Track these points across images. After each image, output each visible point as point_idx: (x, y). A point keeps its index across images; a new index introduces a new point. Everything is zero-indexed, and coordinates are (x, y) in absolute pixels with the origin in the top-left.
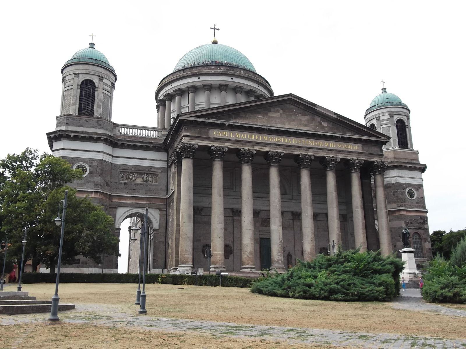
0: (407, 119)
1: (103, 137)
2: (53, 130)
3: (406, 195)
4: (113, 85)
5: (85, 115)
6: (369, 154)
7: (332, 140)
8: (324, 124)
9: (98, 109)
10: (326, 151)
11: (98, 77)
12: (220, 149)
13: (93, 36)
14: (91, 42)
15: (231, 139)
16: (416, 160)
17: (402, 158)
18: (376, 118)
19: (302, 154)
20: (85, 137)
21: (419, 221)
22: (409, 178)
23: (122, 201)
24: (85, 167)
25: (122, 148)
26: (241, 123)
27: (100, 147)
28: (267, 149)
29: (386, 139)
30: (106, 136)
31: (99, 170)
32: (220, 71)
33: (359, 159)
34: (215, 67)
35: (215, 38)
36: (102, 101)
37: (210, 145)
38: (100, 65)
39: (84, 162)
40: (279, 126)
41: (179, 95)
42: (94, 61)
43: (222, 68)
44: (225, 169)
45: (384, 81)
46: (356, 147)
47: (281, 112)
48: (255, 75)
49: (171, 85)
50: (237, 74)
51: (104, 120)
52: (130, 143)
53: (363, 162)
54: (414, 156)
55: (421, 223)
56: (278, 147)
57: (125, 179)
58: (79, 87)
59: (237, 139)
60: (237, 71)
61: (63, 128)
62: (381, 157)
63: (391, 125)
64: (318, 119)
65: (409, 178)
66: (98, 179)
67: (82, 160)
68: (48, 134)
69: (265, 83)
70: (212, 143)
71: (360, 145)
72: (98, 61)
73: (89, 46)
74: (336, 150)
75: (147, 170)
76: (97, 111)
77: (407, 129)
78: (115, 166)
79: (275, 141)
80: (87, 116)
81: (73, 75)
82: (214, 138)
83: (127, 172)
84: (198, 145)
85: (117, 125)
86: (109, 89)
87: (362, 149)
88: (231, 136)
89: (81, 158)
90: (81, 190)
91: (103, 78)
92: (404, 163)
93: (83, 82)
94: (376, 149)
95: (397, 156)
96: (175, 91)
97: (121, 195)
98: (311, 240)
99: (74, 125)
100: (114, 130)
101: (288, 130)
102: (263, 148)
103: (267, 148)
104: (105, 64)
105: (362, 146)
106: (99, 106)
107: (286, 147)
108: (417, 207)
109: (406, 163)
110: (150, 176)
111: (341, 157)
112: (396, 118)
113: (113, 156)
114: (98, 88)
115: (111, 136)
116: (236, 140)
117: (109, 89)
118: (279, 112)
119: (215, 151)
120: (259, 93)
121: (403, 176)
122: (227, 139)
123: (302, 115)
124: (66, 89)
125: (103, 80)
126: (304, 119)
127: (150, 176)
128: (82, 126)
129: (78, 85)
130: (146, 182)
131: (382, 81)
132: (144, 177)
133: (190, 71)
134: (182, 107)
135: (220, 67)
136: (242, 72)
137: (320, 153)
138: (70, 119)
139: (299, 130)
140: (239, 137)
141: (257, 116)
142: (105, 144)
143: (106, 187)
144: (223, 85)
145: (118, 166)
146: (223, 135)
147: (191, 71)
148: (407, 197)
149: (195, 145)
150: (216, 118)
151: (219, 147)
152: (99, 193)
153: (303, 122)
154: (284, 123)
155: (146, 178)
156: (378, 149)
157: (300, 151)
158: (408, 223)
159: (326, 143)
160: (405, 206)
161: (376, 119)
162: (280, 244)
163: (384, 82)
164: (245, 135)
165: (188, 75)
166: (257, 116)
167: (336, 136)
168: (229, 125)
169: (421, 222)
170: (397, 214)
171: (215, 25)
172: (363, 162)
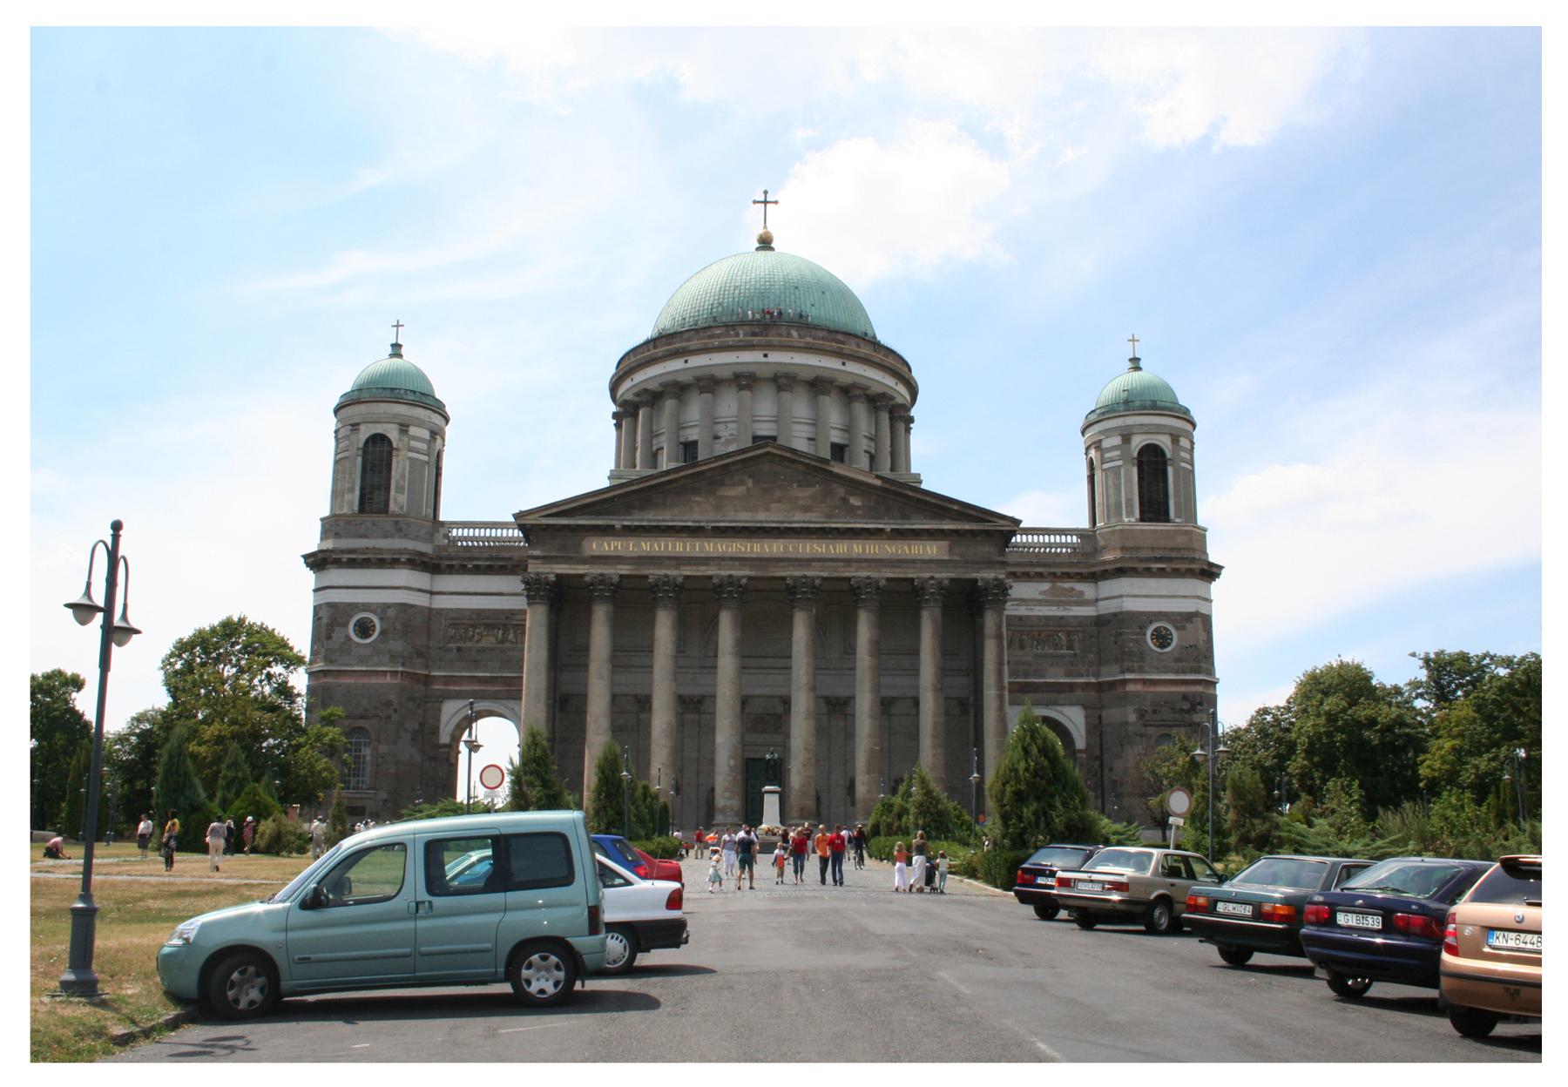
1: (403, 556)
2: (314, 549)
3: (1145, 642)
4: (436, 434)
5: (372, 513)
6: (966, 562)
8: (855, 501)
9: (398, 495)
10: (855, 565)
11: (396, 426)
12: (603, 579)
13: (398, 326)
14: (394, 342)
15: (628, 555)
16: (1184, 549)
17: (1143, 548)
18: (1094, 443)
20: (369, 559)
21: (1178, 707)
22: (1161, 596)
23: (452, 688)
24: (372, 621)
25: (451, 573)
26: (649, 521)
27: (402, 576)
29: (1008, 526)
30: (410, 554)
31: (399, 627)
32: (733, 341)
33: (936, 576)
34: (723, 329)
35: (765, 227)
36: (407, 475)
37: (581, 572)
38: (402, 399)
39: (371, 611)
41: (645, 404)
42: (388, 394)
43: (741, 332)
45: (1136, 338)
46: (932, 549)
47: (750, 483)
48: (833, 335)
49: (630, 378)
50: (776, 343)
52: (465, 563)
53: (946, 582)
54: (1181, 540)
55: (1182, 710)
56: (737, 563)
58: (360, 452)
59: (644, 554)
60: (781, 335)
61: (329, 544)
62: (998, 566)
63: (1124, 463)
64: (841, 491)
65: (1161, 596)
66: (397, 645)
67: (366, 607)
68: (306, 557)
69: (865, 350)
70: (587, 567)
71: (945, 543)
73: (389, 350)
74: (881, 561)
75: (504, 617)
77: (1170, 470)
78: (437, 613)
80: (376, 513)
81: (349, 427)
84: (557, 576)
85: (443, 524)
86: (424, 447)
88: (631, 549)
90: (364, 669)
91: (408, 426)
92: (1141, 560)
93: (367, 442)
94: (986, 549)
95: (1131, 544)
96: (637, 394)
97: (449, 674)
98: (804, 765)
99: (349, 536)
100: (436, 534)
101: (758, 525)
102: (703, 568)
103: (712, 568)
104: (412, 394)
105: (950, 546)
106: (400, 490)
108: (1177, 672)
109: (1149, 560)
110: (512, 631)
112: (1138, 442)
113: (432, 593)
114: (397, 449)
115: (421, 554)
116: (640, 558)
117: (424, 447)
118: (743, 485)
119: (592, 584)
120: (844, 380)
121: (1143, 592)
122: (620, 556)
123: (800, 485)
124: (339, 457)
125: (407, 431)
126: (804, 493)
127: (512, 631)
129: (358, 449)
130: (503, 642)
131: (1131, 338)
133: (666, 345)
134: (655, 434)
135: (737, 328)
136: (794, 333)
137: (839, 569)
138: (342, 523)
139: (783, 522)
141: (693, 499)
142: (412, 569)
143: (418, 661)
144: (742, 376)
145: (443, 612)
146: (612, 549)
147: (670, 344)
148: (1150, 648)
149: (549, 576)
150: (599, 514)
151: (601, 575)
152: (399, 675)
153: (801, 502)
154: (754, 509)
155: (503, 634)
156: (993, 550)
157: (790, 568)
158: (1146, 711)
159: (855, 546)
160: (1141, 670)
161: (1093, 446)
165: (660, 355)
166: (693, 499)
168: (624, 527)
169: (1185, 707)
170: (1119, 690)
171: (766, 192)
172: (946, 582)
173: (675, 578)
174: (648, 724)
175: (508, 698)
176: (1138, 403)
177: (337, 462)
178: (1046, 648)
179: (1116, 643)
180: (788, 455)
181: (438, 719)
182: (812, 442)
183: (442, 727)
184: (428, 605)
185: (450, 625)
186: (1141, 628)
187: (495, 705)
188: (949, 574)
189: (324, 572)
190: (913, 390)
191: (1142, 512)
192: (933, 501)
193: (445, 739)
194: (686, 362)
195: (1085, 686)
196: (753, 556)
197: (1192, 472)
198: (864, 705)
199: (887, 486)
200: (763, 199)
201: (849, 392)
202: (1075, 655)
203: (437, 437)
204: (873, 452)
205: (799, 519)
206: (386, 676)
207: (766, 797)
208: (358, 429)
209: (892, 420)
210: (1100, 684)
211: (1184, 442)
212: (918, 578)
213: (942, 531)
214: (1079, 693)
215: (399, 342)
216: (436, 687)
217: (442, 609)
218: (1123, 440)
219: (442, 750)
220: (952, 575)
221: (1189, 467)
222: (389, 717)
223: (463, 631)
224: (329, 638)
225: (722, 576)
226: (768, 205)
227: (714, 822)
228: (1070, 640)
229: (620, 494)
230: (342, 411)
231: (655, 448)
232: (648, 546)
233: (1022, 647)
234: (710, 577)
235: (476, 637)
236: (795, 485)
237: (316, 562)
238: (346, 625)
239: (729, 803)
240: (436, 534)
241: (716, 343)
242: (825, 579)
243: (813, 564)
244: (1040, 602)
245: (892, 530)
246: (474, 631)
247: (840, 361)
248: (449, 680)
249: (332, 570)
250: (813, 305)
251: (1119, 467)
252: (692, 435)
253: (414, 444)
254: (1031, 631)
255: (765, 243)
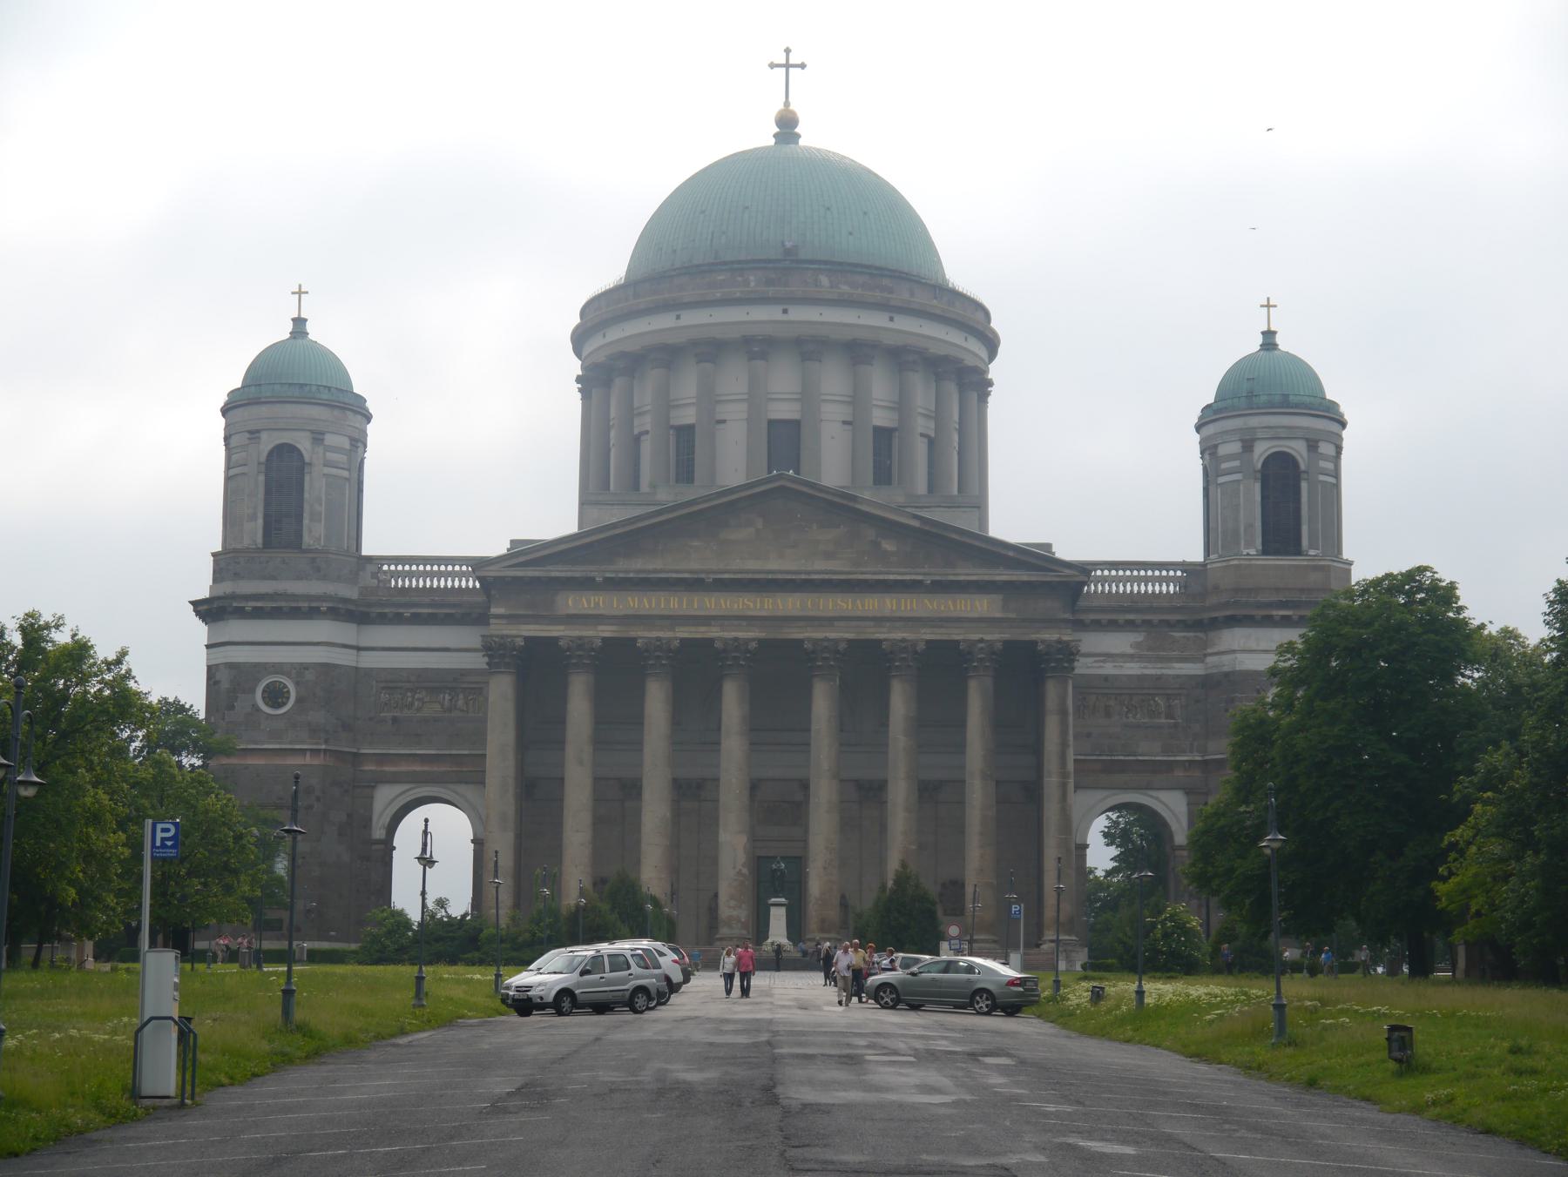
0: (1309, 451)
2: (204, 593)
8: (888, 546)
10: (888, 624)
11: (308, 434)
12: (580, 643)
13: (300, 293)
19: (809, 639)
23: (386, 769)
24: (285, 686)
25: (384, 624)
28: (713, 632)
29: (1076, 576)
36: (324, 498)
39: (282, 673)
40: (752, 565)
43: (752, 278)
44: (600, 697)
46: (982, 605)
51: (330, 556)
52: (401, 611)
56: (744, 623)
57: (395, 708)
58: (263, 468)
59: (630, 612)
61: (227, 587)
67: (278, 668)
68: (195, 603)
70: (562, 628)
71: (997, 598)
72: (308, 388)
76: (310, 531)
77: (1304, 485)
79: (736, 606)
81: (247, 435)
83: (396, 688)
84: (527, 639)
85: (370, 559)
89: (274, 665)
90: (277, 746)
91: (323, 433)
93: (271, 453)
98: (825, 868)
100: (361, 573)
102: (703, 629)
103: (714, 629)
104: (327, 391)
109: (1270, 605)
110: (461, 696)
111: (928, 637)
112: (1262, 450)
114: (310, 464)
115: (345, 601)
116: (626, 617)
119: (569, 649)
124: (232, 472)
125: (323, 440)
127: (461, 696)
128: (273, 578)
129: (259, 463)
130: (450, 710)
132: (444, 698)
134: (635, 412)
136: (824, 280)
140: (636, 606)
146: (592, 605)
151: (580, 638)
155: (451, 700)
162: (736, 880)
163: (1275, 306)
164: (654, 600)
167: (914, 581)
168: (607, 580)
171: (788, 51)
173: (670, 640)
174: (638, 813)
175: (460, 782)
176: (1263, 399)
177: (228, 479)
178: (1138, 716)
179: (1227, 711)
180: (805, 489)
181: (370, 808)
182: (850, 427)
183: (375, 818)
184: (354, 664)
185: (383, 688)
186: (1258, 692)
187: (442, 790)
188: (1003, 635)
189: (221, 624)
190: (991, 344)
191: (1264, 543)
192: (983, 546)
193: (378, 833)
194: (678, 317)
195: (1187, 764)
196: (764, 613)
197: (1337, 487)
198: (899, 793)
199: (927, 528)
200: (784, 62)
201: (902, 357)
202: (1176, 726)
203: (359, 444)
204: (933, 435)
205: (820, 567)
206: (305, 755)
207: (773, 910)
208: (259, 438)
209: (962, 388)
210: (1206, 762)
211: (1326, 449)
212: (964, 641)
213: (993, 583)
214: (1179, 773)
215: (302, 316)
216: (366, 768)
217: (372, 669)
218: (1243, 447)
219: (374, 847)
220: (1006, 636)
221: (1332, 480)
222: (310, 807)
223: (400, 696)
224: (232, 707)
225: (726, 639)
226: (791, 70)
227: (717, 936)
228: (1170, 706)
229: (603, 539)
230: (230, 413)
231: (636, 431)
232: (636, 603)
233: (1108, 714)
234: (712, 640)
235: (416, 703)
236: (815, 526)
237: (207, 610)
238: (253, 691)
239: (735, 913)
240: (361, 573)
241: (718, 295)
242: (849, 641)
243: (836, 623)
244: (1131, 657)
246: (413, 697)
247: (886, 316)
248: (382, 759)
249: (231, 621)
250: (851, 234)
251: (1238, 481)
252: (687, 416)
253: (331, 456)
254: (1121, 694)
255: (787, 125)
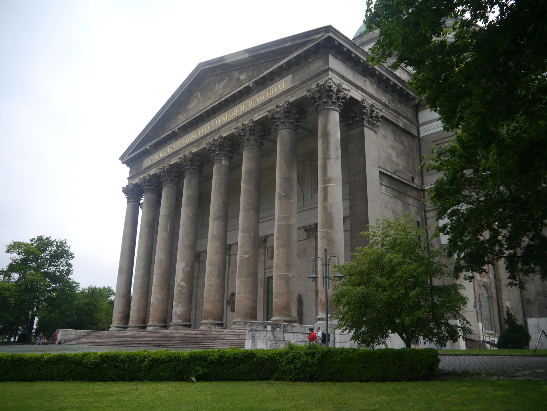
7: (249, 96)
10: (240, 120)
29: (323, 36)
56: (191, 147)
71: (289, 78)
82: (144, 169)
87: (292, 81)
107: (197, 143)
245: (253, 83)
